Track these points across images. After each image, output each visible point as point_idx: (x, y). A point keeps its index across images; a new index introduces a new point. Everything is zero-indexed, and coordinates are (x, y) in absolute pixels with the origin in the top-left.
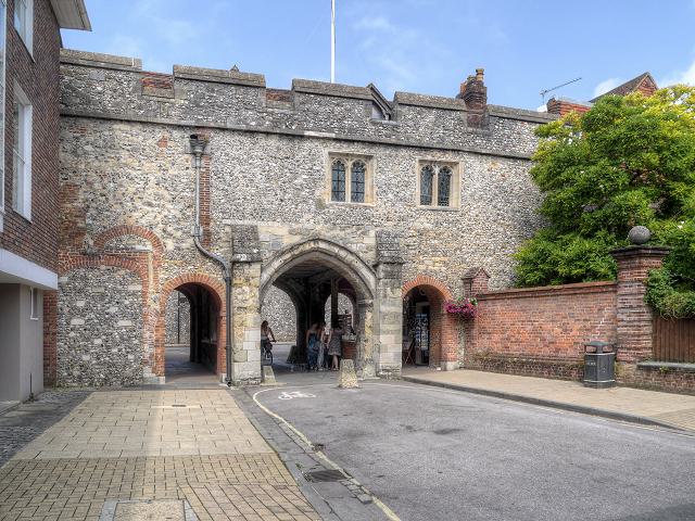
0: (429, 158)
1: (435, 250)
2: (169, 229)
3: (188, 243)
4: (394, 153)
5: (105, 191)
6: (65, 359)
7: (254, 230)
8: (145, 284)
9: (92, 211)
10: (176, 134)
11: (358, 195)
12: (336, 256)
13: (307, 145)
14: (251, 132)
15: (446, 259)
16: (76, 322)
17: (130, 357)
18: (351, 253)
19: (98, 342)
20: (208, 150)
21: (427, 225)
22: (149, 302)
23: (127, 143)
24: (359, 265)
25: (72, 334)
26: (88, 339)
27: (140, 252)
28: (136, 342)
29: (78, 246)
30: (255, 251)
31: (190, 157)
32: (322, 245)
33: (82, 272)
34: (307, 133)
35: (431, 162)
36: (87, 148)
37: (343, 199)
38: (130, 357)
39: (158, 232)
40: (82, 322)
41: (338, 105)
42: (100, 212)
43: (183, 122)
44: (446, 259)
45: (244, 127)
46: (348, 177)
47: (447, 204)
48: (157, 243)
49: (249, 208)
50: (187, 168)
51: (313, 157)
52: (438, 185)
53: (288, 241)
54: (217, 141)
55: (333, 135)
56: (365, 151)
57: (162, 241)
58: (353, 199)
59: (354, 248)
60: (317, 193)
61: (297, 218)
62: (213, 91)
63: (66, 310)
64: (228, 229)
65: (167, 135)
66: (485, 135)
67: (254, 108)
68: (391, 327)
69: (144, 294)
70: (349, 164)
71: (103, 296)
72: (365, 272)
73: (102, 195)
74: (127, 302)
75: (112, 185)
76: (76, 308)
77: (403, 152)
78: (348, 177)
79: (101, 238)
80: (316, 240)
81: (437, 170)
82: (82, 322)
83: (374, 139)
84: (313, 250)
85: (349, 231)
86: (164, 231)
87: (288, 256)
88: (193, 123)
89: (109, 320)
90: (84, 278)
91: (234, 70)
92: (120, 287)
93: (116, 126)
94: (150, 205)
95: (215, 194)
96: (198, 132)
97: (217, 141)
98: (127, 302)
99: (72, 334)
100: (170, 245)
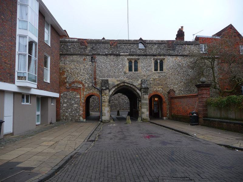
0: (156, 58)
1: (159, 84)
2: (86, 81)
3: (91, 85)
4: (145, 57)
6: (62, 114)
7: (107, 80)
8: (80, 95)
9: (68, 78)
10: (88, 57)
11: (136, 70)
12: (130, 87)
13: (121, 57)
14: (106, 55)
15: (162, 87)
16: (65, 105)
17: (77, 114)
18: (134, 86)
19: (69, 110)
20: (95, 60)
21: (156, 77)
24: (136, 89)
25: (64, 108)
27: (79, 87)
29: (65, 86)
31: (91, 62)
32: (126, 84)
33: (66, 93)
35: (157, 59)
37: (132, 71)
38: (77, 114)
39: (83, 82)
42: (70, 78)
43: (89, 54)
44: (162, 87)
46: (133, 66)
47: (163, 71)
48: (83, 85)
51: (123, 60)
52: (159, 66)
53: (117, 83)
54: (98, 58)
55: (128, 54)
56: (137, 57)
57: (84, 84)
58: (135, 71)
59: (135, 84)
60: (124, 70)
61: (119, 76)
63: (62, 102)
64: (101, 81)
65: (85, 57)
66: (173, 50)
67: (107, 49)
68: (145, 107)
69: (80, 98)
70: (133, 61)
71: (71, 99)
72: (138, 91)
73: (70, 73)
74: (76, 100)
77: (148, 57)
78: (133, 66)
79: (70, 84)
80: (124, 83)
81: (159, 61)
83: (140, 54)
84: (123, 85)
85: (133, 80)
87: (117, 87)
88: (91, 54)
89: (72, 105)
90: (67, 94)
91: (104, 39)
93: (74, 56)
94: (82, 75)
95: (97, 72)
96: (93, 56)
97: (98, 58)
98: (76, 100)
99: (64, 108)
100: (86, 85)
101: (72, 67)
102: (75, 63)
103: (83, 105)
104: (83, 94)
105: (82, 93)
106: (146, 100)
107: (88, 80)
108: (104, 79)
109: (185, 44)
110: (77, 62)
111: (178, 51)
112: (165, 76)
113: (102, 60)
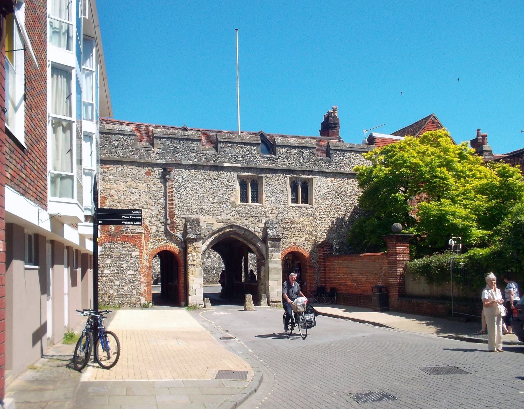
2: (153, 221)
5: (120, 200)
7: (197, 220)
8: (141, 250)
10: (156, 169)
14: (195, 167)
17: (134, 291)
19: (117, 283)
22: (143, 261)
23: (130, 174)
26: (111, 281)
27: (138, 233)
28: (137, 283)
30: (199, 233)
33: (108, 245)
34: (225, 165)
36: (111, 177)
38: (134, 291)
40: (109, 272)
41: (241, 148)
43: (159, 161)
45: (191, 163)
49: (195, 208)
50: (161, 187)
55: (239, 165)
60: (232, 198)
62: (174, 143)
64: (184, 220)
71: (119, 258)
73: (119, 202)
74: (132, 261)
75: (123, 196)
76: (105, 264)
80: (232, 226)
82: (109, 272)
86: (150, 222)
87: (216, 235)
90: (110, 248)
92: (128, 253)
95: (176, 201)
98: (132, 261)
100: (154, 229)
101: (121, 189)
102: (129, 180)
103: (147, 271)
104: (147, 249)
105: (145, 246)
106: (277, 263)
107: (156, 219)
108: (190, 216)
109: (351, 151)
110: (134, 177)
111: (337, 164)
112: (312, 214)
113: (186, 177)
